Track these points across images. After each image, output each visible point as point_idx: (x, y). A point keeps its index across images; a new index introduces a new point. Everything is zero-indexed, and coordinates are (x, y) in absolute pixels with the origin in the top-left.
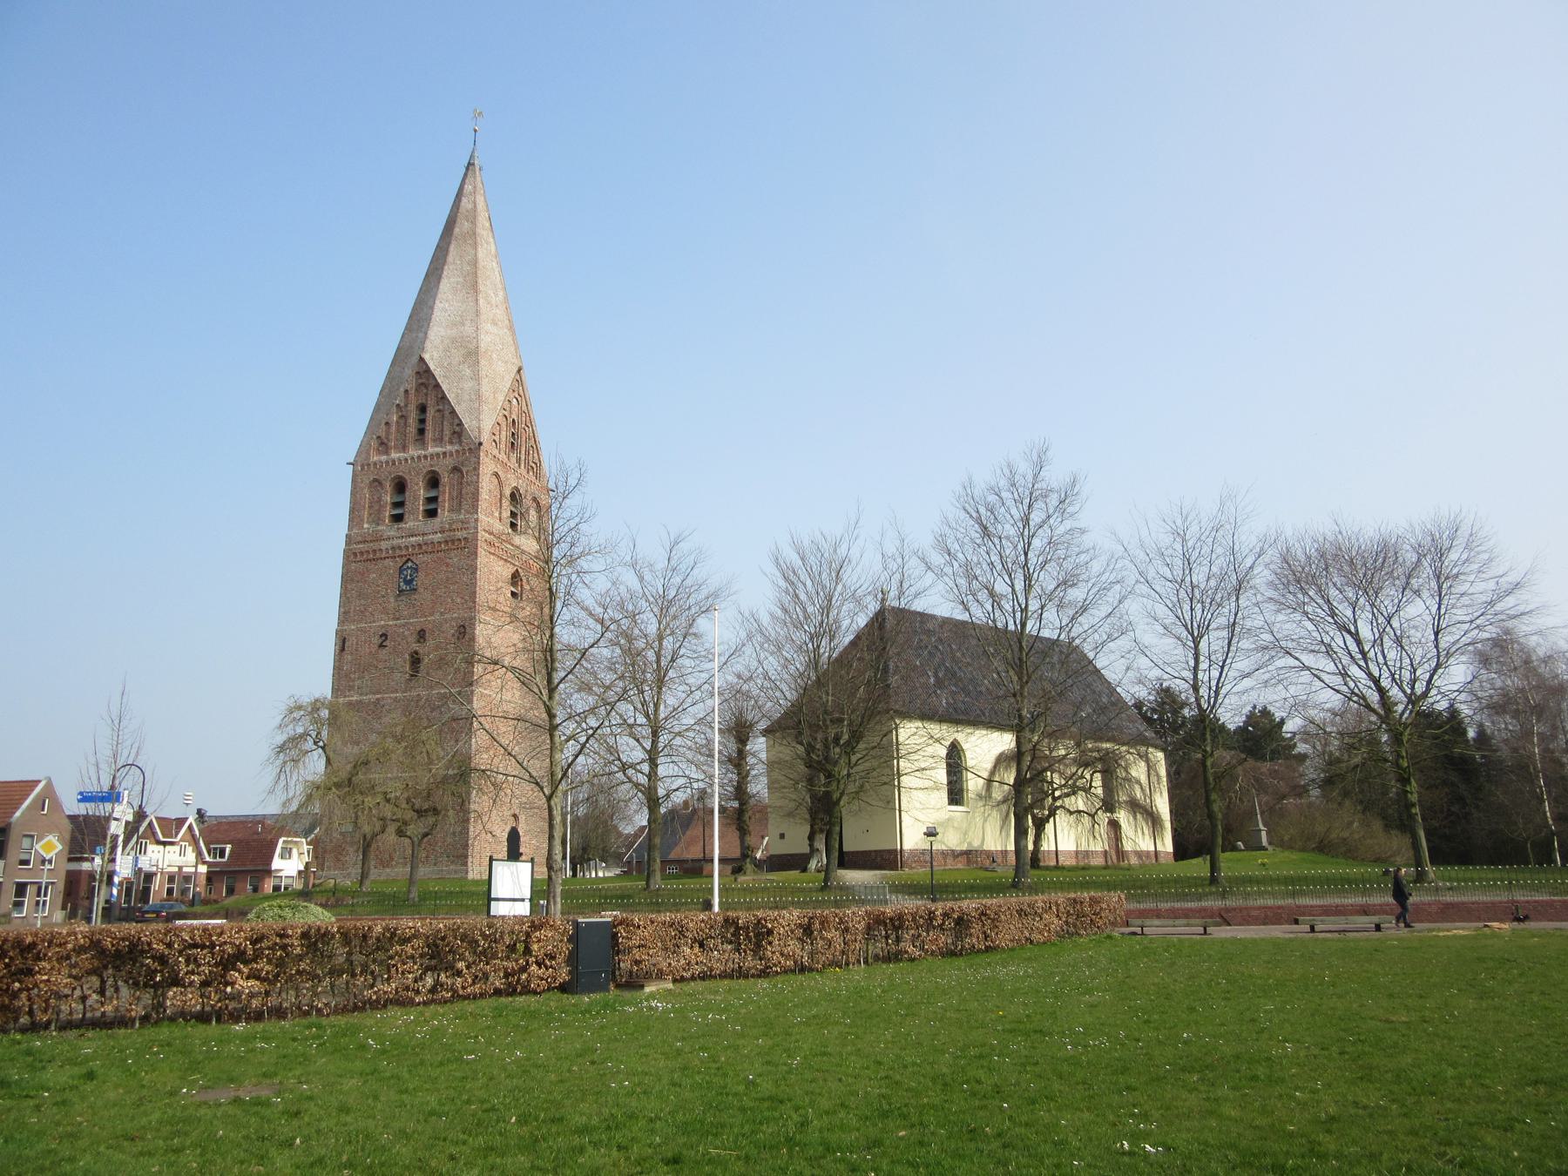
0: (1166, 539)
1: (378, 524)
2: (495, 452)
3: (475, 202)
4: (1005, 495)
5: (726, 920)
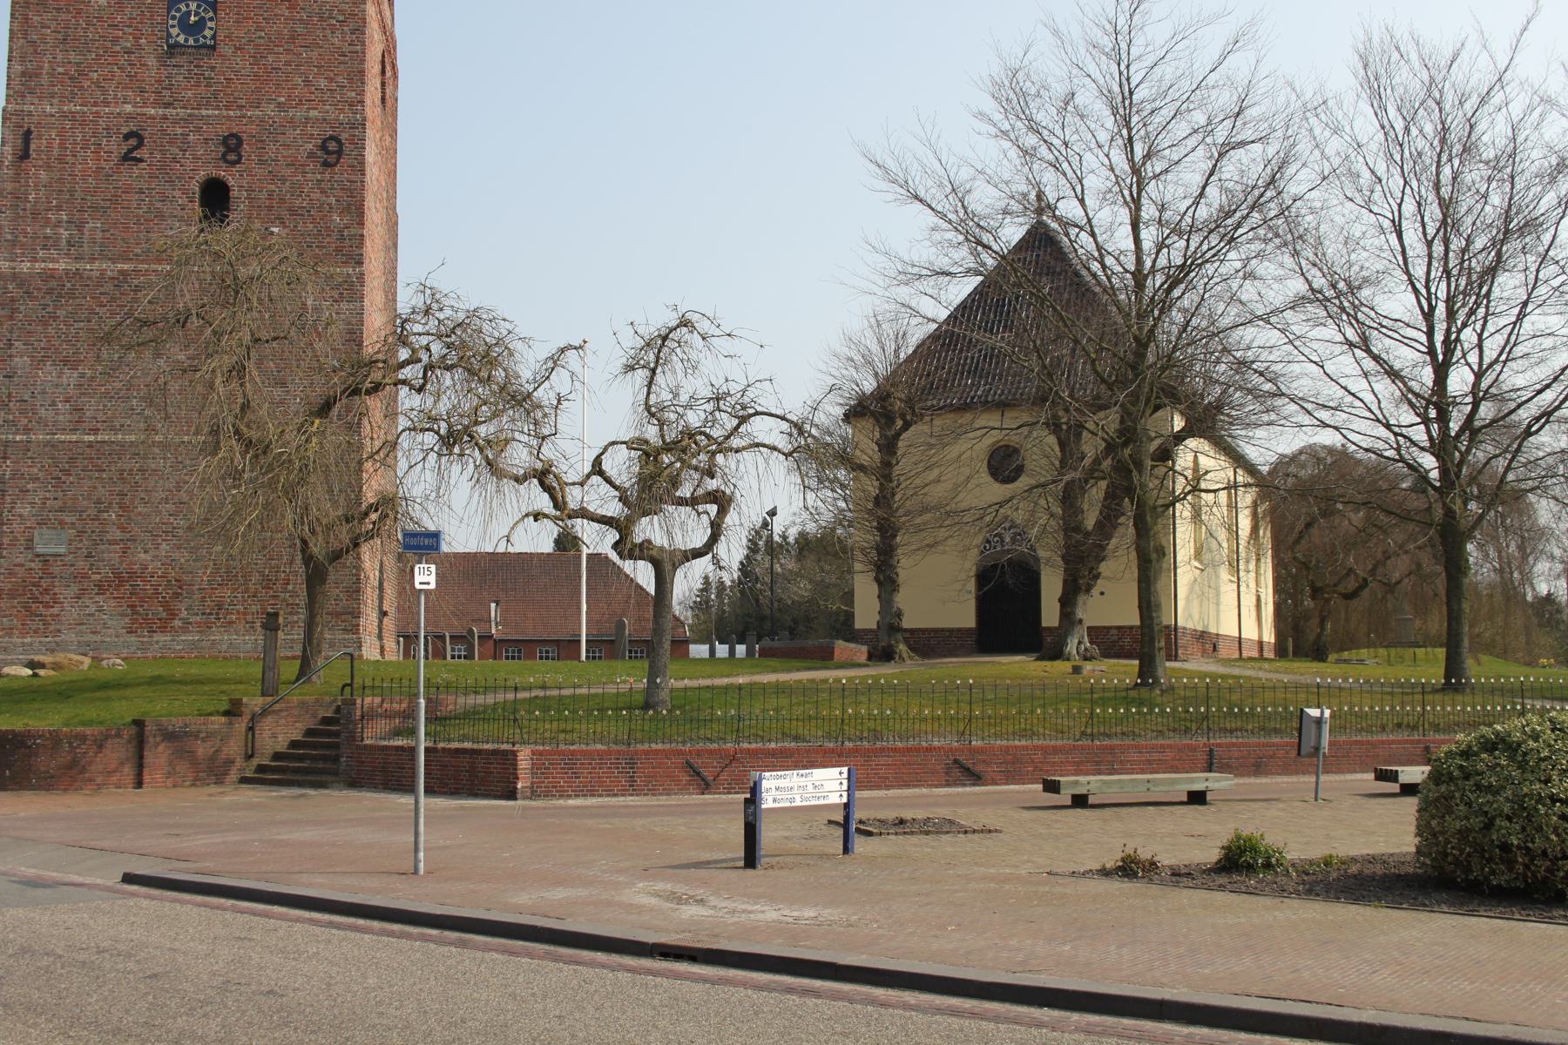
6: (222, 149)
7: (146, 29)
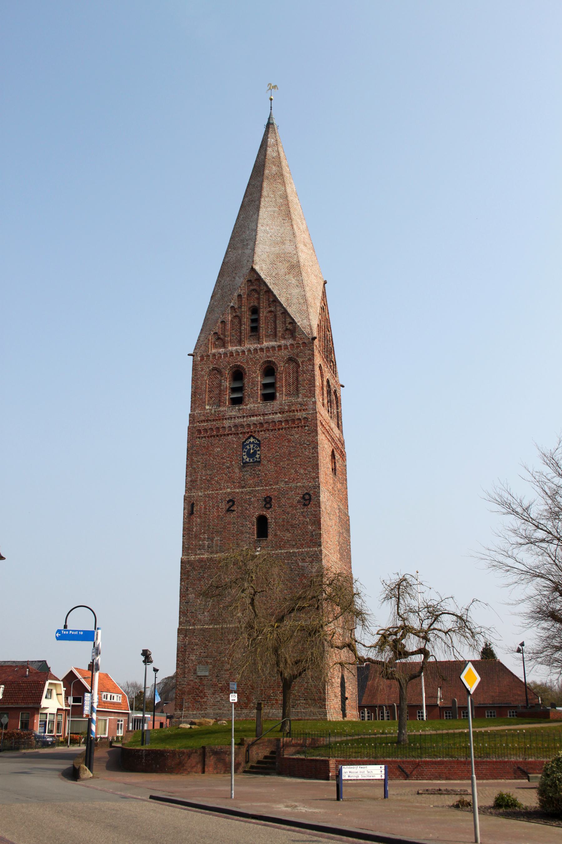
1: (220, 406)
3: (278, 151)
6: (264, 503)
7: (234, 458)
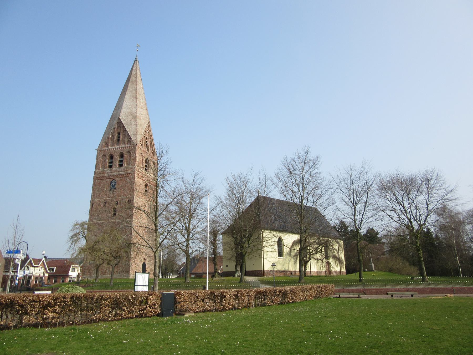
0: (346, 176)
1: (104, 169)
2: (141, 147)
4: (297, 161)
5: (211, 293)
